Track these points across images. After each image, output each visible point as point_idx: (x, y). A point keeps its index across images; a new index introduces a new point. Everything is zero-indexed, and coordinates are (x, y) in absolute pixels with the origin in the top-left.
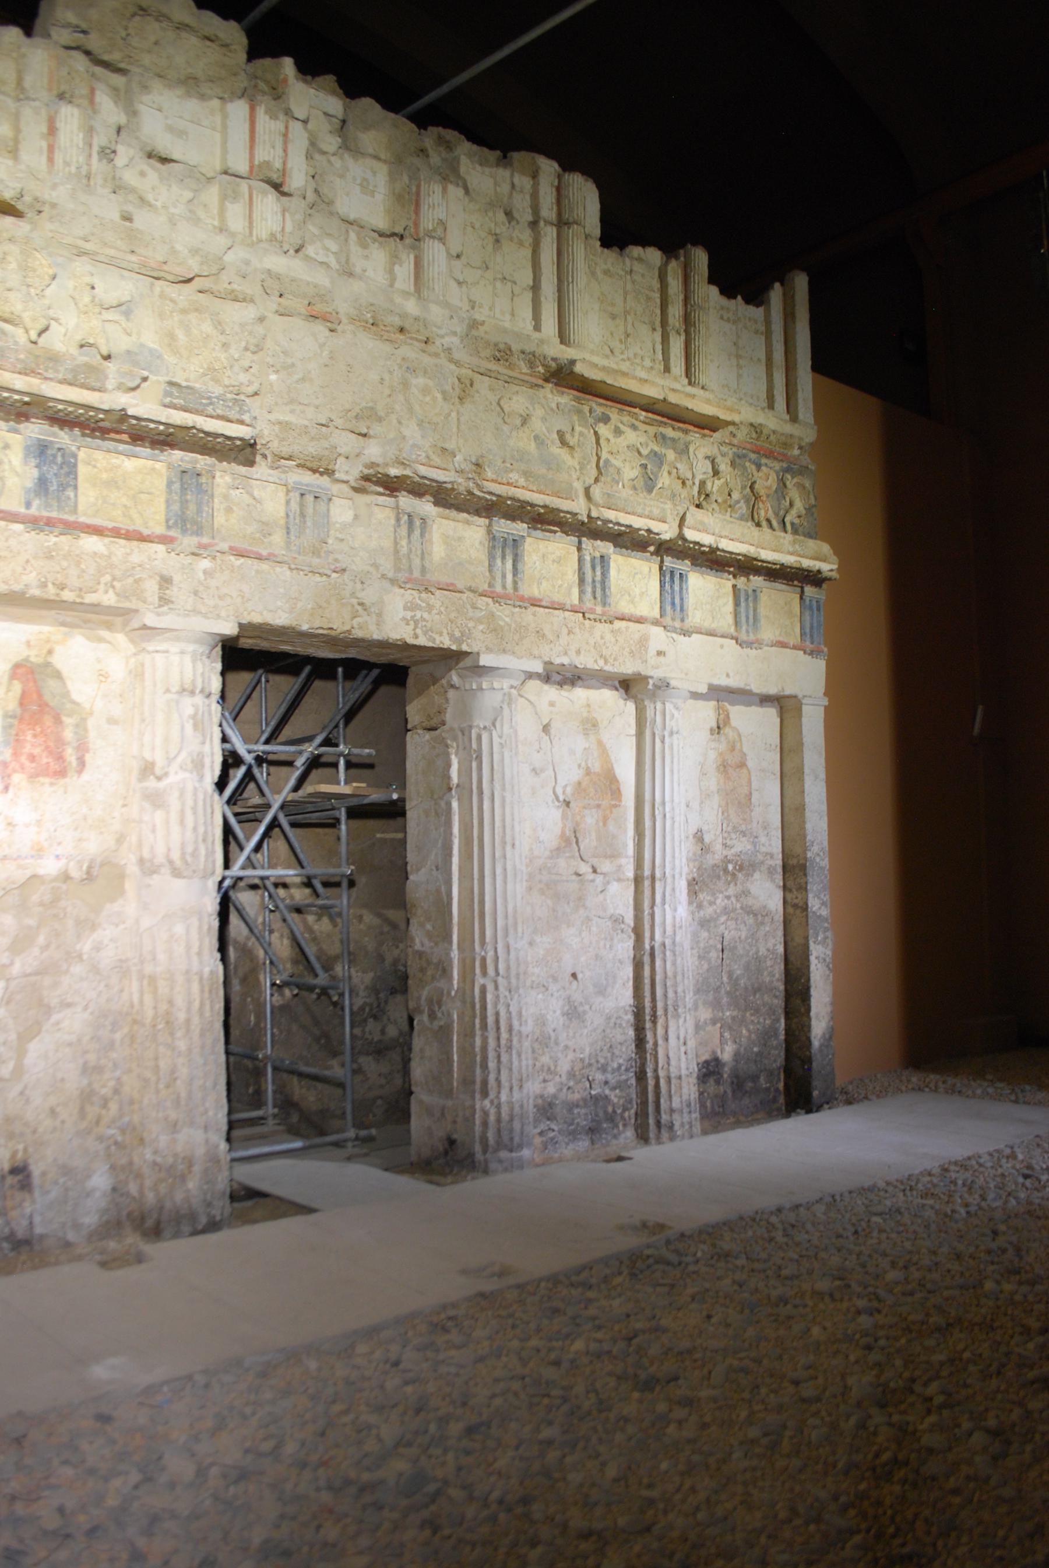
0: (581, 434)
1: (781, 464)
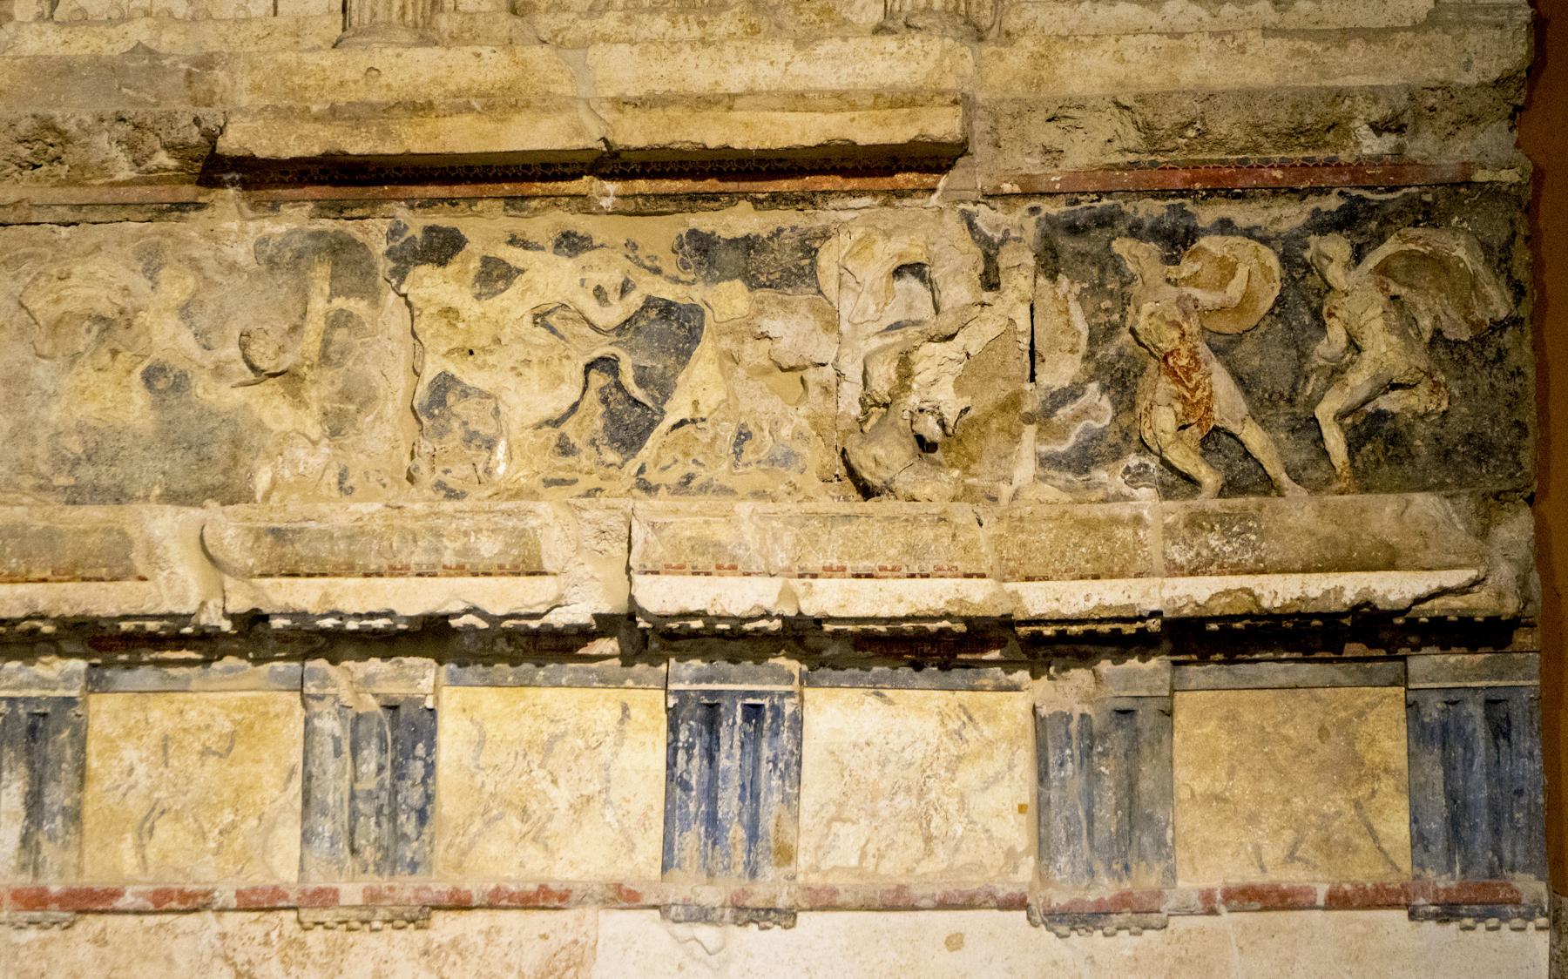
0: (339, 320)
1: (1313, 203)
